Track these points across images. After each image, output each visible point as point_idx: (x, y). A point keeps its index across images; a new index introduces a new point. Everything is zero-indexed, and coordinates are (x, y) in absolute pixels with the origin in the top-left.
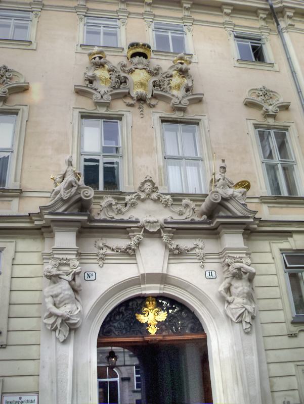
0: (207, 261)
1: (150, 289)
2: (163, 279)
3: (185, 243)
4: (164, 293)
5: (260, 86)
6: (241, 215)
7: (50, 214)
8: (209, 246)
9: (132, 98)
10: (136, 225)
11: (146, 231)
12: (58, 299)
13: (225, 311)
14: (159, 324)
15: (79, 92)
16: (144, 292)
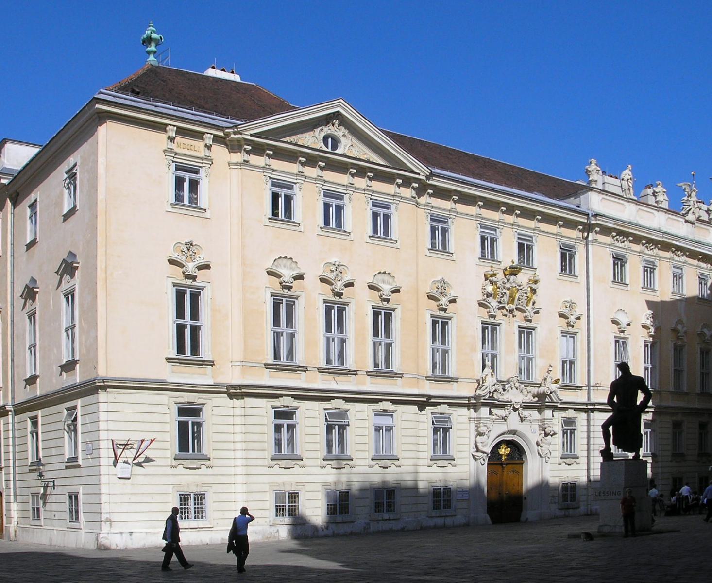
0: (533, 423)
1: (508, 437)
2: (514, 432)
3: (526, 413)
4: (513, 440)
5: (568, 299)
6: (555, 401)
7: (484, 400)
8: (535, 414)
9: (507, 310)
10: (510, 403)
11: (514, 407)
12: (484, 444)
13: (538, 450)
14: (508, 455)
15: (481, 305)
16: (505, 439)
